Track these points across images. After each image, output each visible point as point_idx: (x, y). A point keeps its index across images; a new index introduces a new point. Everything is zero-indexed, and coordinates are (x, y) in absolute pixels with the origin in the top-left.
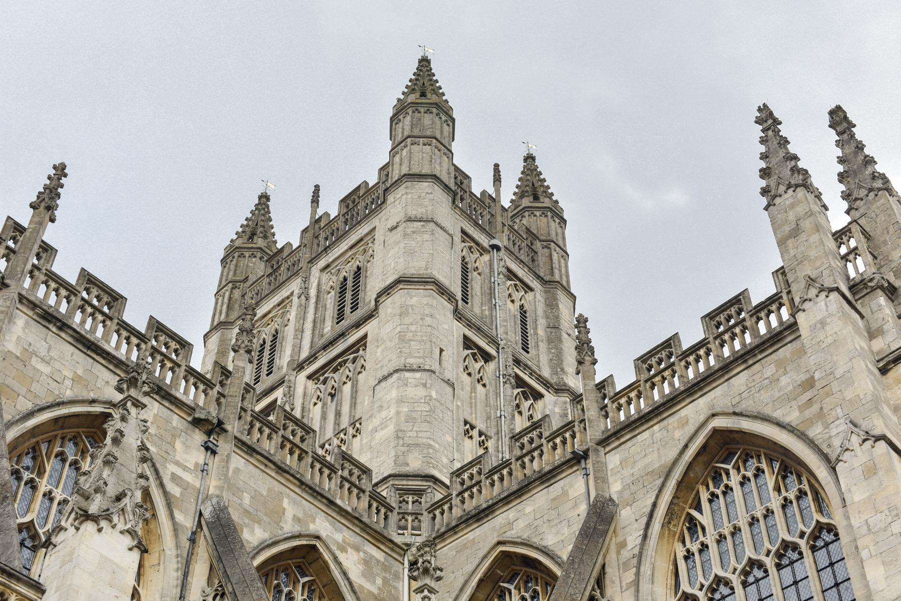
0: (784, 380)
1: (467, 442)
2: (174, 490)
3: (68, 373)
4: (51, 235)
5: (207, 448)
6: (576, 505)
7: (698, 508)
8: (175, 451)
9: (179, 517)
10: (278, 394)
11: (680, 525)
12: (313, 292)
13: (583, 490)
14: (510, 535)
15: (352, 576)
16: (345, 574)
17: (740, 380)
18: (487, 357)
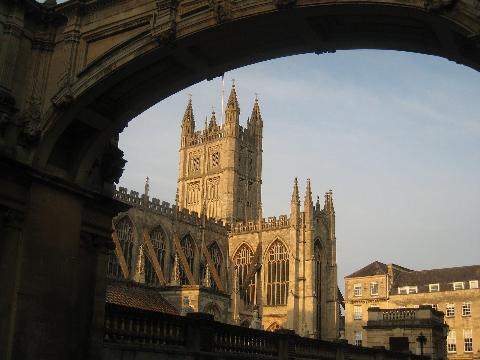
0: (288, 236)
1: (239, 203)
2: (198, 241)
3: (184, 229)
4: (179, 204)
5: (201, 232)
6: (256, 241)
7: (273, 248)
8: (197, 234)
9: (199, 246)
10: (201, 179)
11: (271, 250)
12: (207, 153)
13: (257, 238)
14: (246, 240)
15: (221, 244)
16: (219, 244)
17: (282, 231)
18: (243, 180)
